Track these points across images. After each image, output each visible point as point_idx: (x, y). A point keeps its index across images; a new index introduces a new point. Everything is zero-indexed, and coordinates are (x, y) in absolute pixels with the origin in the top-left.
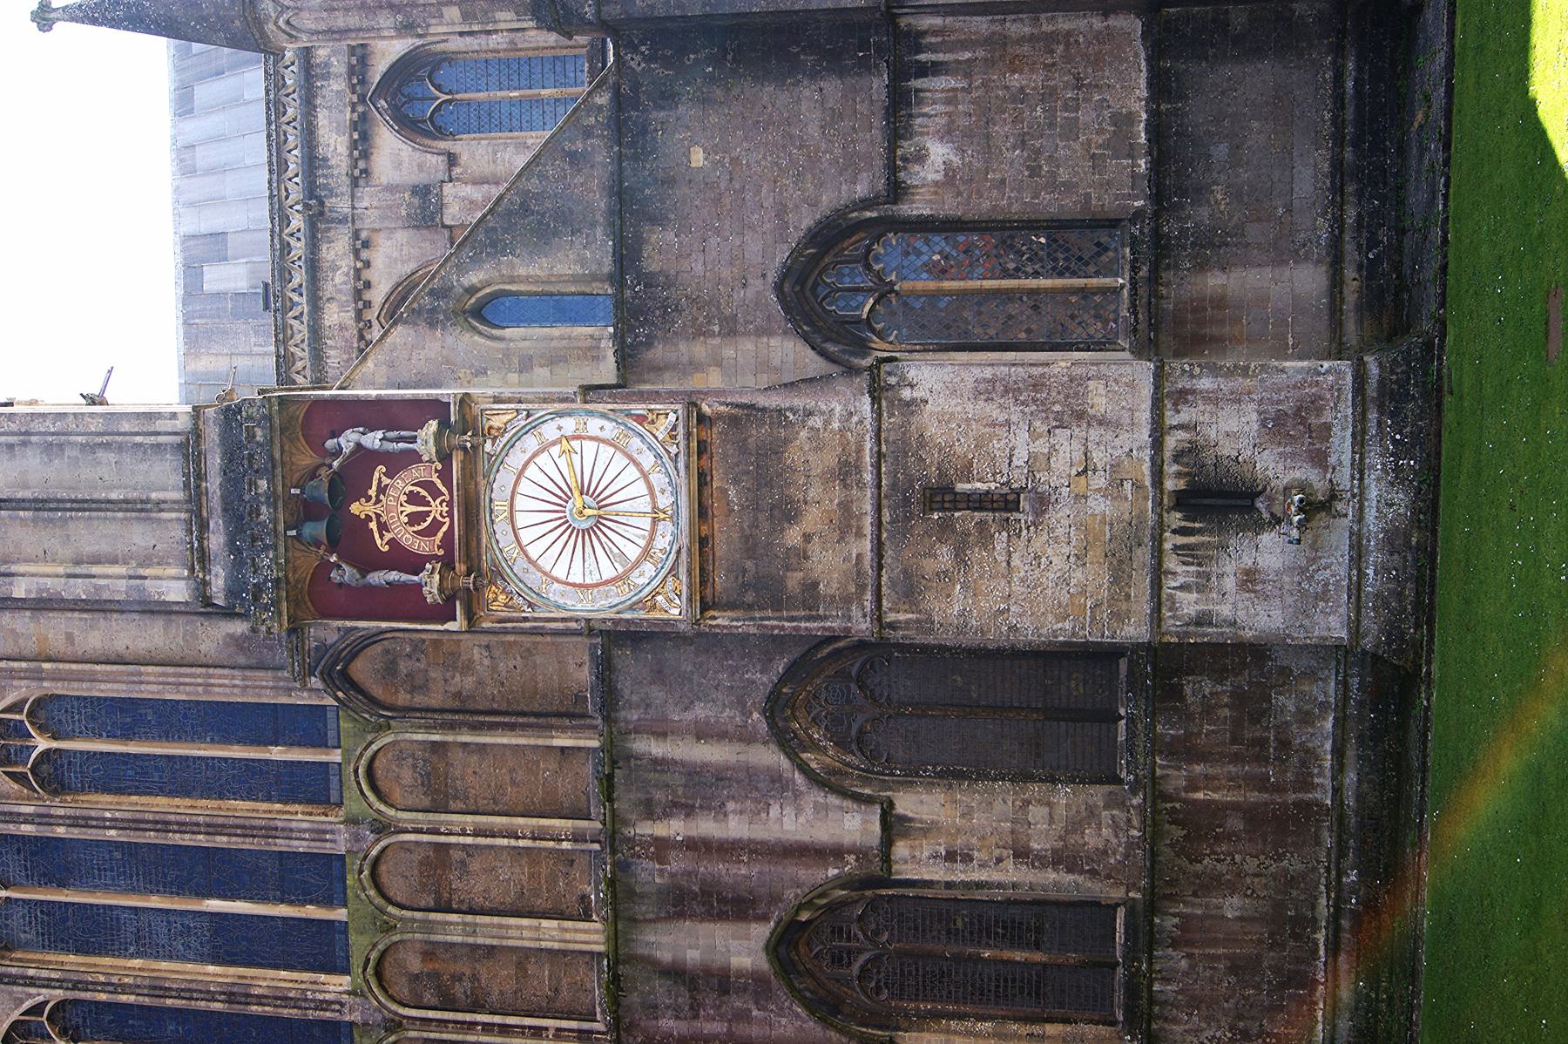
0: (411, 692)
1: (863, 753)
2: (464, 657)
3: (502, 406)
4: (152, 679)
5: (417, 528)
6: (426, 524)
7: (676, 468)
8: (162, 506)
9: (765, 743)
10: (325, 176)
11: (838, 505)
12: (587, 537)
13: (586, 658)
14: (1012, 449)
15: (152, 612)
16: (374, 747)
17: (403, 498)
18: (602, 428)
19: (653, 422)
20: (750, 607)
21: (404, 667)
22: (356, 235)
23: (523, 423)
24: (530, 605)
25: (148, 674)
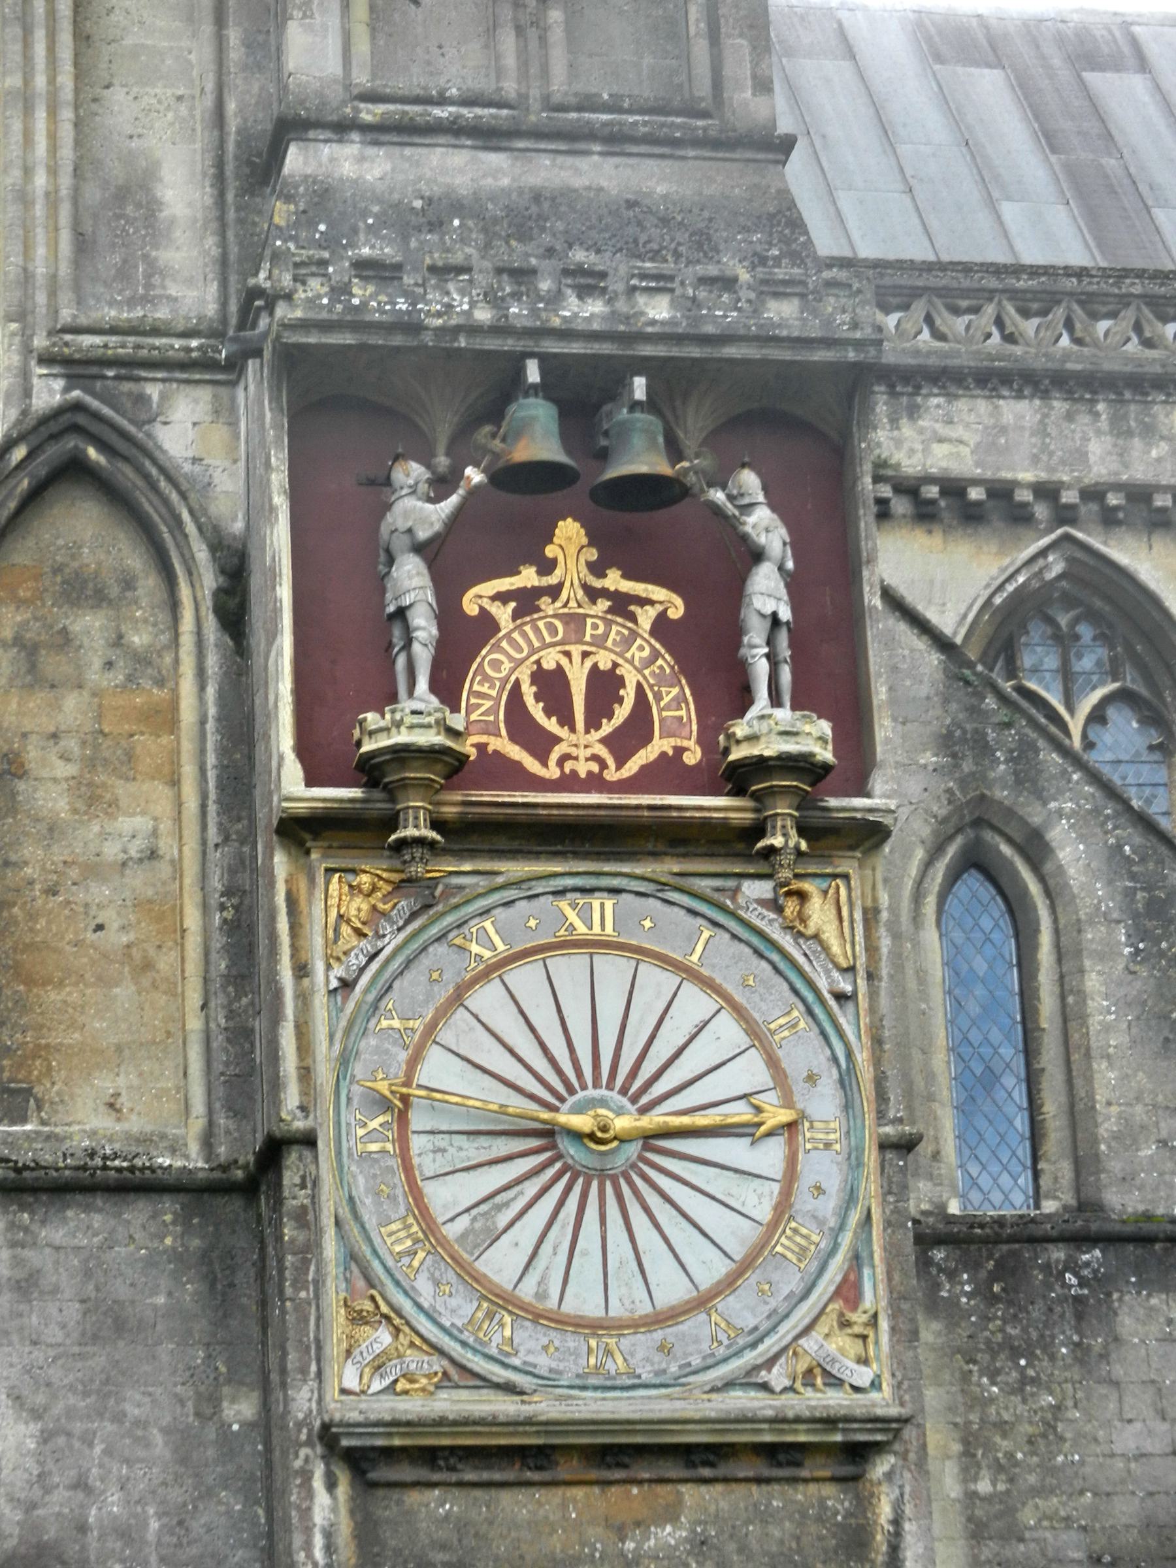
2: (121, 789)
5: (528, 691)
7: (729, 1384)
8: (533, 33)
12: (534, 1143)
13: (135, 1124)
17: (604, 660)
18: (819, 1190)
19: (845, 1324)
23: (823, 984)
24: (347, 985)
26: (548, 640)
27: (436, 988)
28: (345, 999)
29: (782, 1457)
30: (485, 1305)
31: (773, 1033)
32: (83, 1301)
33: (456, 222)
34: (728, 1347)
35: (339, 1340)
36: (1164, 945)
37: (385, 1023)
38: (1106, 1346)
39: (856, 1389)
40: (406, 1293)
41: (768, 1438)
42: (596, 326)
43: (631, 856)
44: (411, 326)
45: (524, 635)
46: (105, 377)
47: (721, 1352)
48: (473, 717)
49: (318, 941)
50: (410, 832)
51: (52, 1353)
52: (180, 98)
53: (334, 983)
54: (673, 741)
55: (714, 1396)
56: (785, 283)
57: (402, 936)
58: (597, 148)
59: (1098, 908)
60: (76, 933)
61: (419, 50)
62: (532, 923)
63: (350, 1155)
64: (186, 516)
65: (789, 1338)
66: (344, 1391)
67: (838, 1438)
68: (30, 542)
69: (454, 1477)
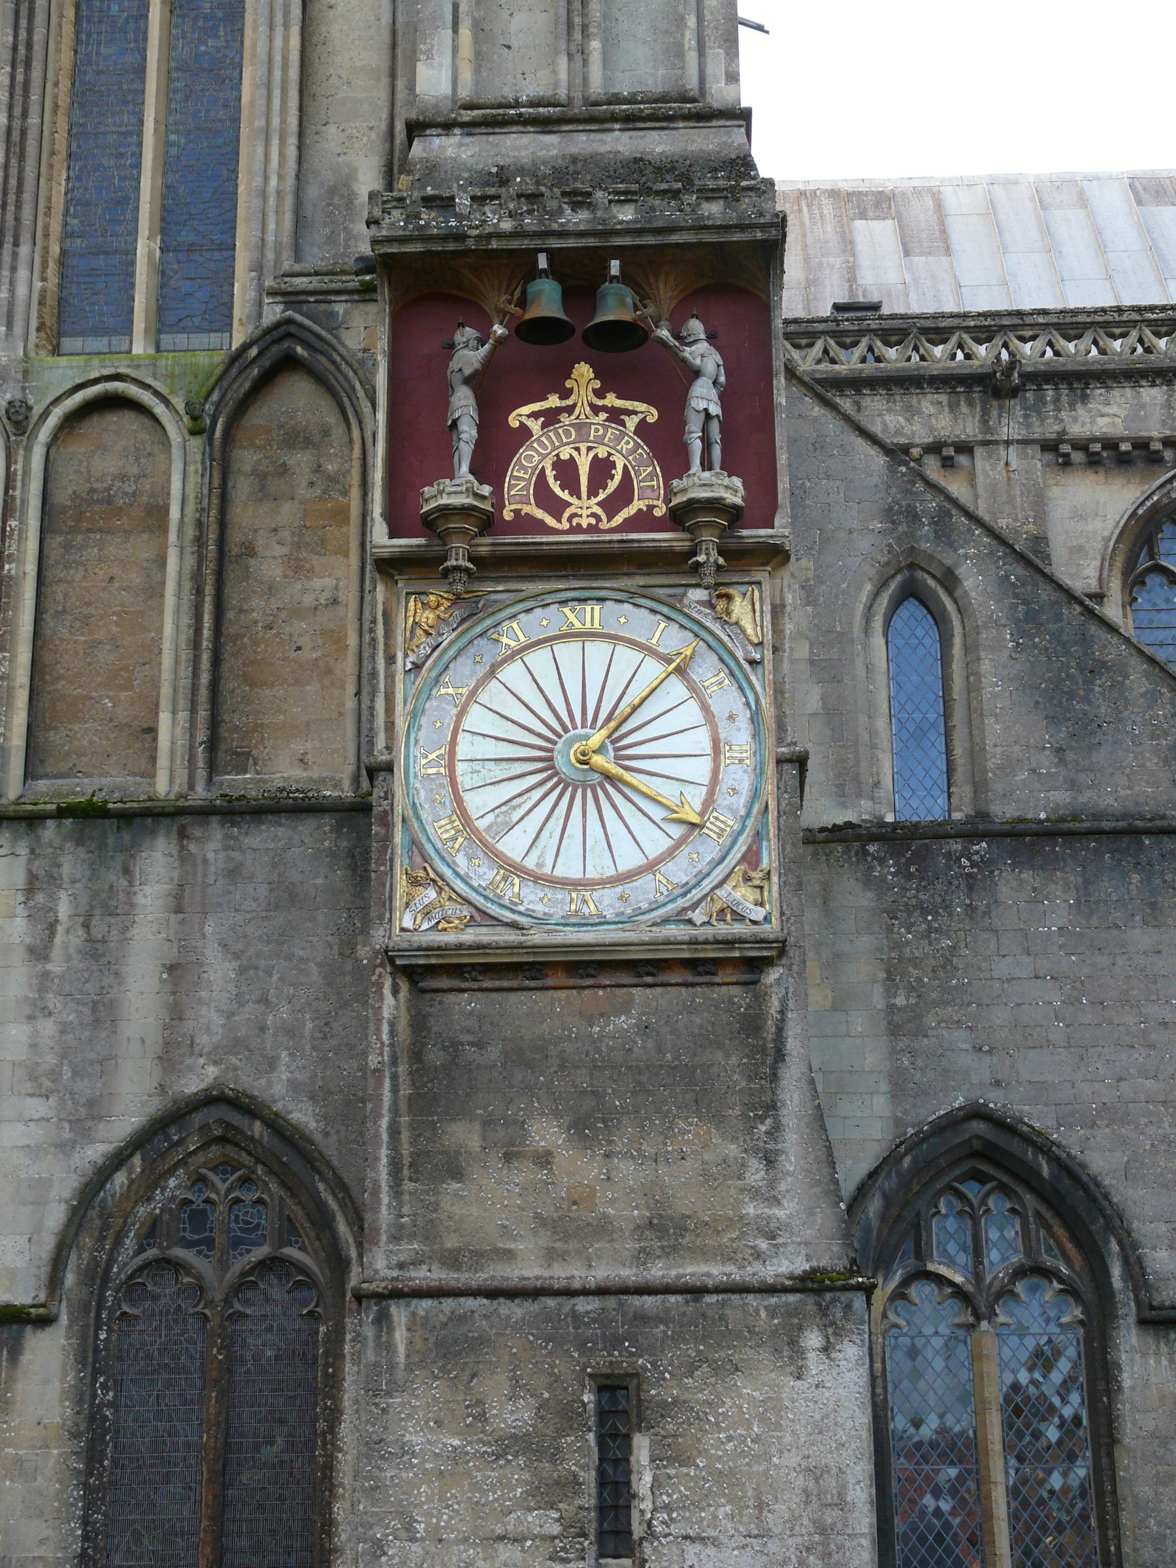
0: (254, 472)
1: (140, 1270)
2: (316, 561)
3: (768, 618)
4: (278, 43)
5: (550, 474)
6: (557, 490)
7: (665, 921)
8: (578, 58)
9: (162, 1088)
10: (1057, 400)
11: (605, 1216)
12: (540, 765)
13: (315, 773)
14: (715, 1542)
15: (394, 46)
16: (159, 409)
17: (602, 452)
19: (747, 879)
20: (417, 1056)
21: (300, 461)
22: (965, 448)
23: (740, 655)
24: (417, 667)
25: (286, 39)
26: (565, 440)
27: (478, 667)
28: (416, 678)
29: (700, 969)
30: (502, 872)
31: (706, 688)
32: (269, 883)
33: (518, 179)
34: (667, 896)
35: (401, 896)
36: (1037, 640)
37: (443, 691)
38: (988, 906)
39: (754, 922)
40: (449, 865)
41: (687, 955)
42: (582, 227)
43: (614, 576)
44: (460, 237)
45: (549, 438)
46: (309, 302)
47: (662, 899)
48: (512, 493)
49: (400, 639)
50: (452, 562)
51: (248, 916)
52: (371, 128)
53: (409, 666)
54: (646, 502)
55: (654, 929)
56: (713, 190)
57: (455, 633)
58: (617, 126)
59: (991, 617)
60: (283, 653)
61: (509, 77)
62: (545, 623)
63: (416, 776)
64: (358, 386)
65: (708, 889)
66: (403, 930)
67: (737, 954)
68: (265, 410)
69: (476, 985)
